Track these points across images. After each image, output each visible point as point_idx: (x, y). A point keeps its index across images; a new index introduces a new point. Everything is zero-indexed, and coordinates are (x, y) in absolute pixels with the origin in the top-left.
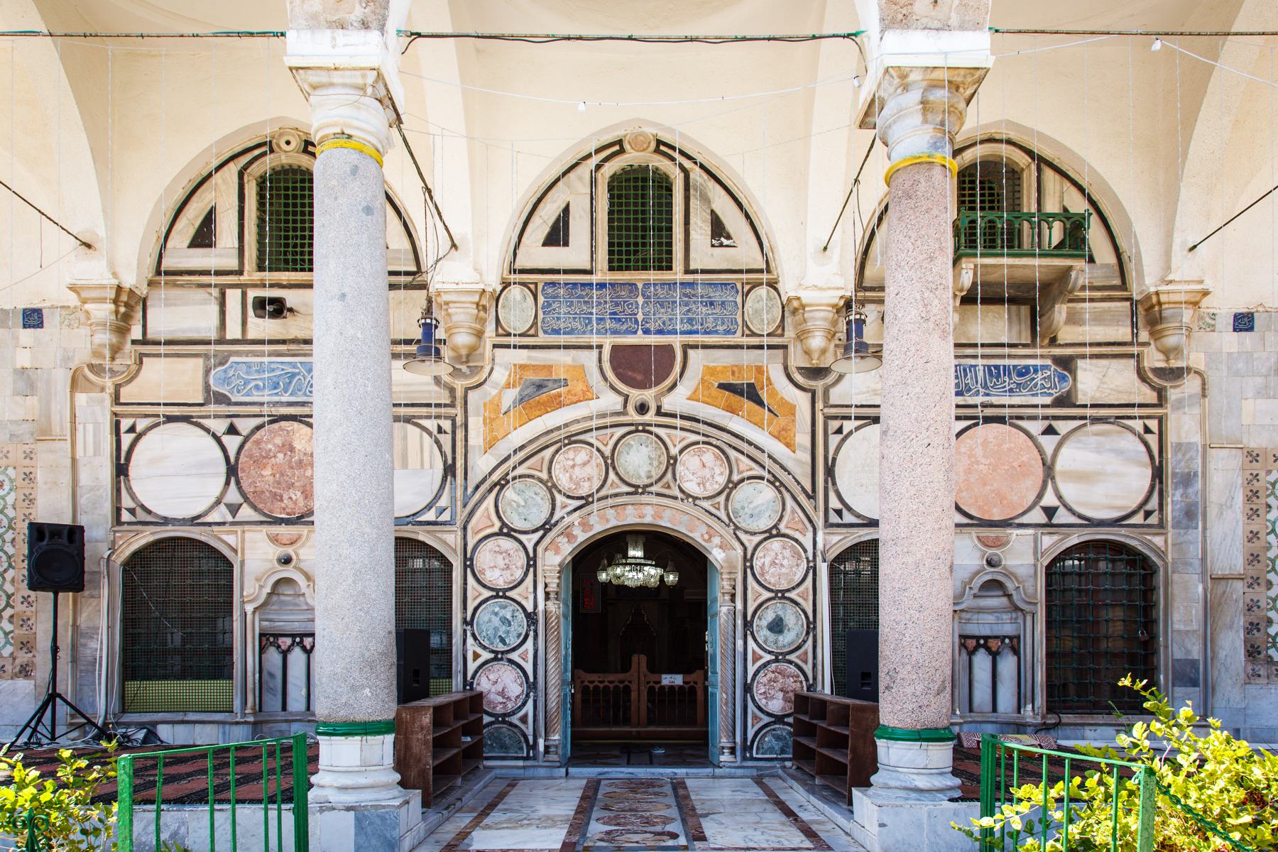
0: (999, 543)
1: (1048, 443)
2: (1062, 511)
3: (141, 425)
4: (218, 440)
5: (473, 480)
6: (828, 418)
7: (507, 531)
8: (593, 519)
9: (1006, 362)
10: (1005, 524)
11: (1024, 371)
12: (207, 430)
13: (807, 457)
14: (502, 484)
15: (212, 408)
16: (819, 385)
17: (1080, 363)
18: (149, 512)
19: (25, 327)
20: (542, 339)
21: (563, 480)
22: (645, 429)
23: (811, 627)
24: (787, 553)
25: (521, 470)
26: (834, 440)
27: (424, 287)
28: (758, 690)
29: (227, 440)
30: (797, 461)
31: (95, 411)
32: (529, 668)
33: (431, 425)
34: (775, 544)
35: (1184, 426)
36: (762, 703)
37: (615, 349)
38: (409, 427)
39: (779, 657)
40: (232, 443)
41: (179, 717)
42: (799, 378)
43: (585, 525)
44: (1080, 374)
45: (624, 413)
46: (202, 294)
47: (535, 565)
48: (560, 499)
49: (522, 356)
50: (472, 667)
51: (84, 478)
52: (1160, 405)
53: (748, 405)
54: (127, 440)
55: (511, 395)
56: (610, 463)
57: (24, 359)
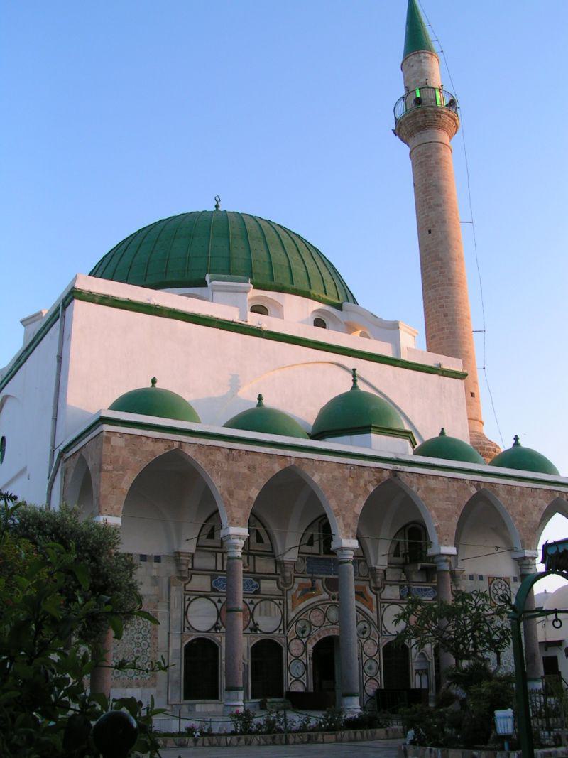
3: (192, 598)
4: (215, 604)
5: (290, 619)
6: (381, 603)
7: (298, 638)
9: (423, 587)
11: (426, 590)
12: (212, 600)
13: (376, 615)
14: (297, 621)
15: (213, 593)
18: (193, 628)
19: (155, 562)
21: (313, 620)
22: (334, 605)
23: (379, 668)
24: (372, 644)
25: (302, 617)
26: (383, 609)
27: (274, 556)
28: (367, 688)
29: (217, 604)
30: (374, 616)
31: (176, 593)
32: (305, 682)
33: (277, 601)
34: (369, 642)
36: (367, 692)
37: (326, 579)
39: (372, 678)
40: (219, 605)
41: (203, 701)
42: (373, 590)
43: (319, 636)
45: (329, 599)
46: (209, 554)
47: (306, 649)
48: (313, 627)
49: (300, 580)
50: (289, 683)
51: (174, 616)
53: (361, 598)
54: (187, 603)
55: (299, 593)
56: (326, 616)
57: (154, 573)
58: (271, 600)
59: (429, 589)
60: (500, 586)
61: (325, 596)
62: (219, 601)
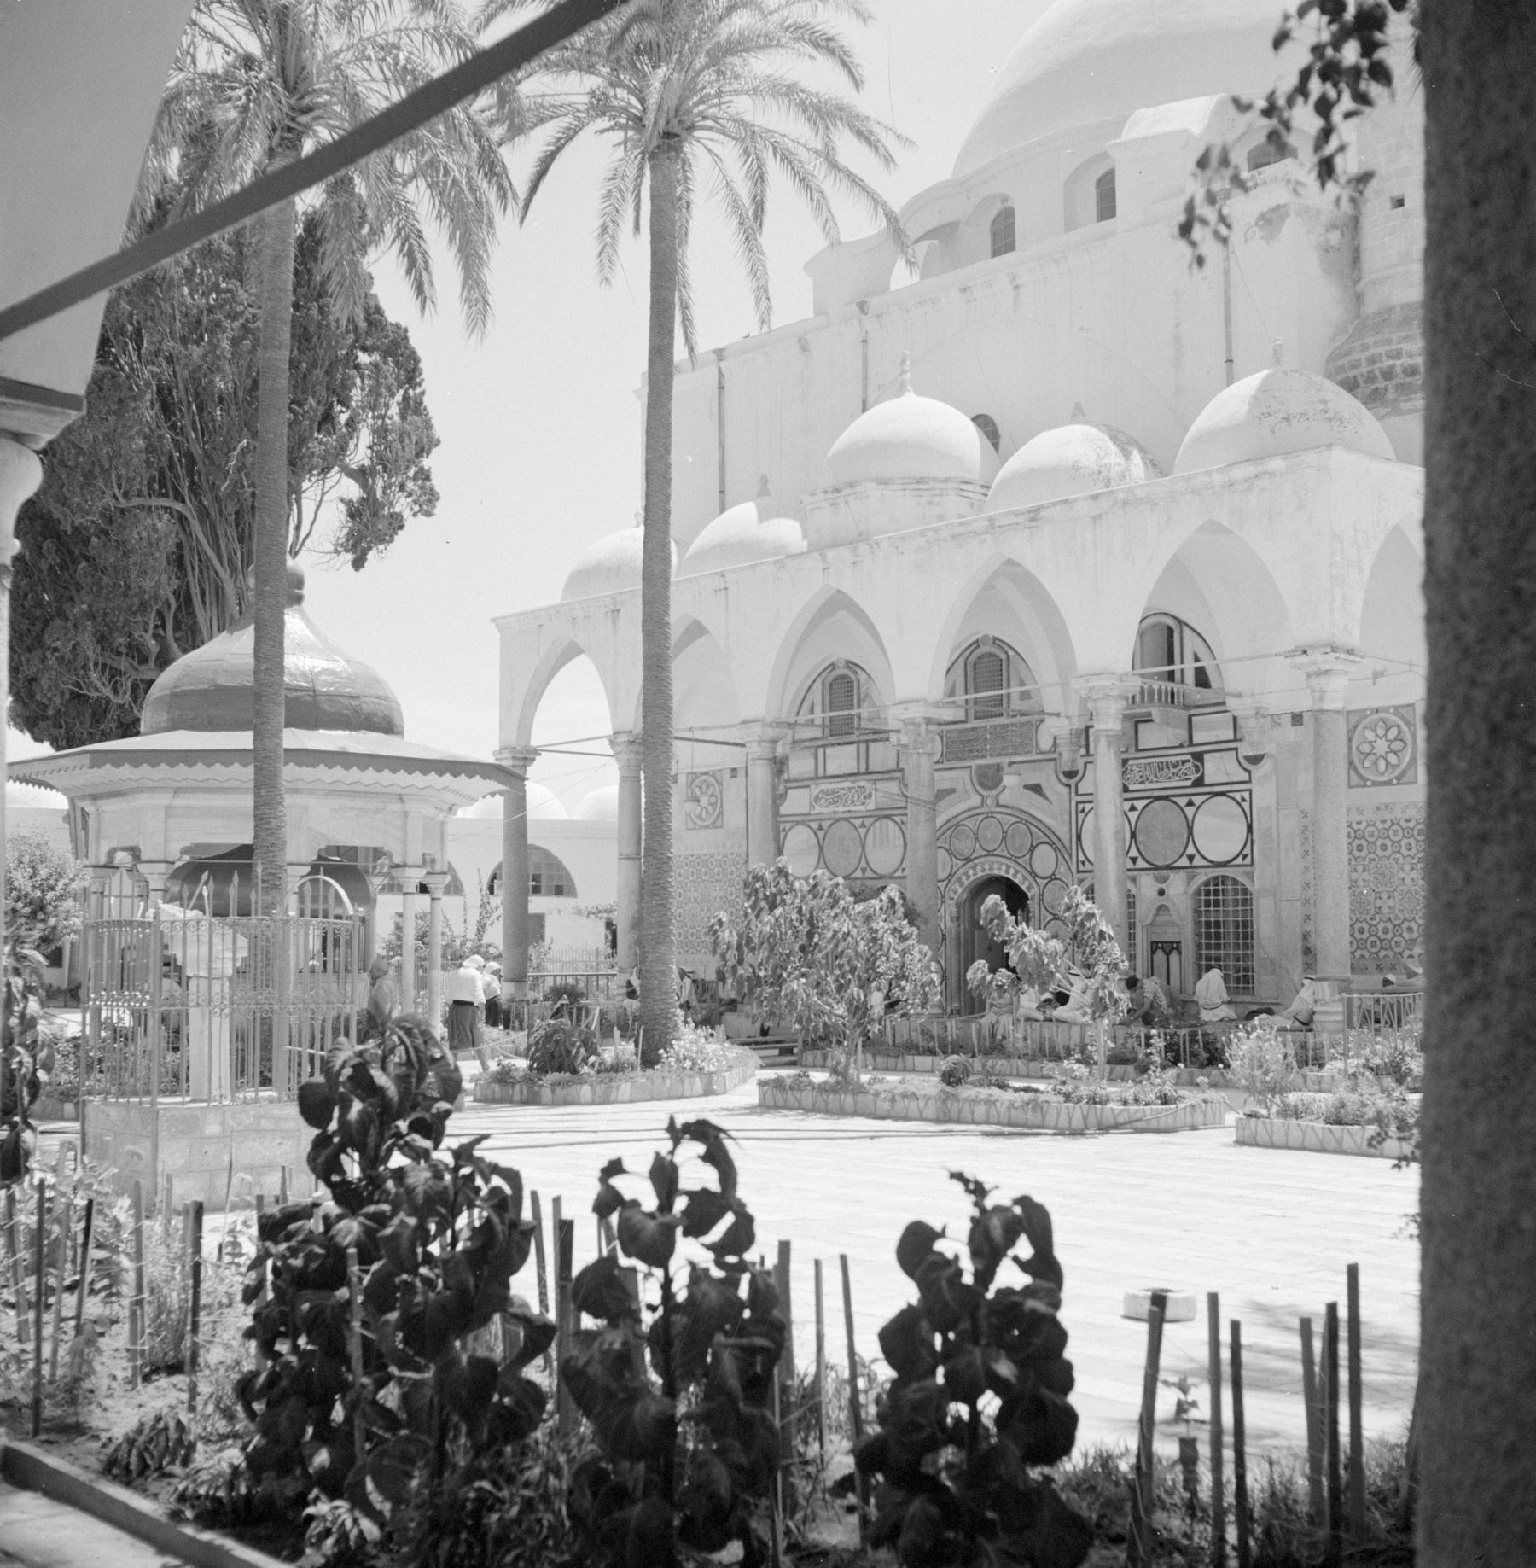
0: (1165, 879)
1: (1190, 811)
2: (1198, 857)
8: (971, 872)
10: (1168, 867)
16: (1072, 782)
17: (1206, 756)
20: (946, 765)
26: (1081, 816)
33: (897, 819)
35: (1263, 795)
38: (891, 824)
40: (821, 834)
42: (1064, 779)
44: (1206, 764)
52: (1250, 781)
58: (889, 817)
59: (1184, 762)
60: (1381, 732)
61: (975, 800)
62: (821, 828)
